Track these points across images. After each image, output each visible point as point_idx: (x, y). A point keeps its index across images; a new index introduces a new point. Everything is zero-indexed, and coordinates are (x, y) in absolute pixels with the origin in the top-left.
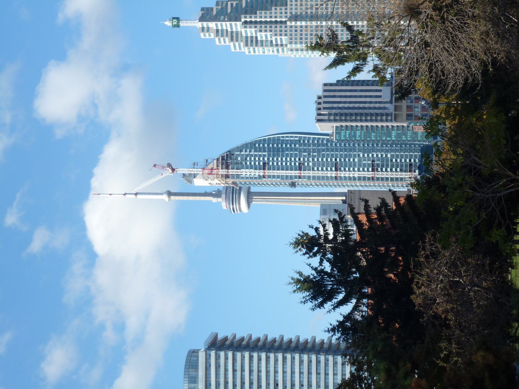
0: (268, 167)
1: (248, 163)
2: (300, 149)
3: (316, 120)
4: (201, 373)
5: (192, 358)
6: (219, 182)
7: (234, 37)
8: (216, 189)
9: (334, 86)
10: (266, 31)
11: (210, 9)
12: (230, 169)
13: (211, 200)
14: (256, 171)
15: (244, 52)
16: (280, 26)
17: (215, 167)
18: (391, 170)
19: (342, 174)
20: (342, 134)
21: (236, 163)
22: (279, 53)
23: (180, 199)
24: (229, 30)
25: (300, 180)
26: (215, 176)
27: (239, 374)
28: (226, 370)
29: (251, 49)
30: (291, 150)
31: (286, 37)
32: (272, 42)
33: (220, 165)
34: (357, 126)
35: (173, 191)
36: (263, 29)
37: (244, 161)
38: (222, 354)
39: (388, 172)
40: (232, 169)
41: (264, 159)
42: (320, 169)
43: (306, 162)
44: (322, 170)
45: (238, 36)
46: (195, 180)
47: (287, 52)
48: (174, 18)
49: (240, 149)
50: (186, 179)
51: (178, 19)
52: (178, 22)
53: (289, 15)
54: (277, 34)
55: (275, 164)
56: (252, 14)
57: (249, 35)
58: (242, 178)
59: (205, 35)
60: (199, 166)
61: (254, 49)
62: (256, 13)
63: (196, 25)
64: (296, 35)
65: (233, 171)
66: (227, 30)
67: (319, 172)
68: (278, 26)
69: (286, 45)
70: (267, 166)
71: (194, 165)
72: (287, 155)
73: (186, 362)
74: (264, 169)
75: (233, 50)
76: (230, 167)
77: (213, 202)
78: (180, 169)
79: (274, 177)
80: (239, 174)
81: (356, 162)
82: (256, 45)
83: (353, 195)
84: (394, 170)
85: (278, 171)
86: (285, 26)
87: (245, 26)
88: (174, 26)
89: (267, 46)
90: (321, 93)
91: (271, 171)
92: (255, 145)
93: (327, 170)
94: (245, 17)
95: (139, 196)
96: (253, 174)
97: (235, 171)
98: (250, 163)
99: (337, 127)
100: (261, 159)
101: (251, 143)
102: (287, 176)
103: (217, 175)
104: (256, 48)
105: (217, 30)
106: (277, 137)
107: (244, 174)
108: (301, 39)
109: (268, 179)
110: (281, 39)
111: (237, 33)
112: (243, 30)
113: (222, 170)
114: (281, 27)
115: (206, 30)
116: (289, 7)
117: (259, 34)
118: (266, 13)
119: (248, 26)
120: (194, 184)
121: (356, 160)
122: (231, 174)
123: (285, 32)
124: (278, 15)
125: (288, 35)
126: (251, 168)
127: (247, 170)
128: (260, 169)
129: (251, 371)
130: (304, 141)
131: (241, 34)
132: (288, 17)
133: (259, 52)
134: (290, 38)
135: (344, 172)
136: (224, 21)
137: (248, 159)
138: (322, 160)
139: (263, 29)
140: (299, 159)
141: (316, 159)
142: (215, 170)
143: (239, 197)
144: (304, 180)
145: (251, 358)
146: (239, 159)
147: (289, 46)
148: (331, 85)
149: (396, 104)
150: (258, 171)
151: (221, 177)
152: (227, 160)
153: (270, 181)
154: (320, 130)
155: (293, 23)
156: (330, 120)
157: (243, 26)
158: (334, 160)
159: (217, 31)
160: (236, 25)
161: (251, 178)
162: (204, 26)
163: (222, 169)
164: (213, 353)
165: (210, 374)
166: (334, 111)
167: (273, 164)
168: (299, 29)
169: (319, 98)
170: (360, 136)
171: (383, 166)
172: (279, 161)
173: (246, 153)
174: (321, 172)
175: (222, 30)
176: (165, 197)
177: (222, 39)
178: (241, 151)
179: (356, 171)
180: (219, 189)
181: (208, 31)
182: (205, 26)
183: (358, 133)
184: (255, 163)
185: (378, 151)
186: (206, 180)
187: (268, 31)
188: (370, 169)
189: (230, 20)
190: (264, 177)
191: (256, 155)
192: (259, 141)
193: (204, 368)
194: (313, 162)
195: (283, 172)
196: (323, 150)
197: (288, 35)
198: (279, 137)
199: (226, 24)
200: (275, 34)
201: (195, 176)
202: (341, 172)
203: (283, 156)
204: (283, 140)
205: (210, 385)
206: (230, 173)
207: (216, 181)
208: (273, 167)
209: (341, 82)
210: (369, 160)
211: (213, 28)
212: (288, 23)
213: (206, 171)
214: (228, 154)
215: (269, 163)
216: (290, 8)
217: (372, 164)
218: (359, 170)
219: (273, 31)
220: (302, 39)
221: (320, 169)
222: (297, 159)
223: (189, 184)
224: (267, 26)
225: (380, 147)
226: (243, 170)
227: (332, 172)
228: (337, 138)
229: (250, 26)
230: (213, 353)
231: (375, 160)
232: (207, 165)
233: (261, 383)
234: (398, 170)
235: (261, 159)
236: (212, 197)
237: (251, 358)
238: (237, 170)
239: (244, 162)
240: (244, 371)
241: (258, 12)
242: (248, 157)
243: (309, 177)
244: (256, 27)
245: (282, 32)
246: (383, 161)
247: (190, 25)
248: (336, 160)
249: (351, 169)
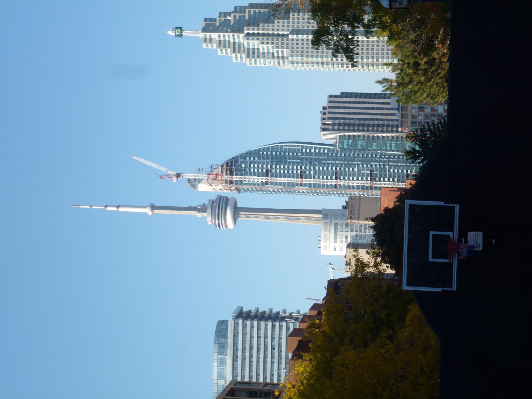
0: (271, 174)
1: (252, 170)
2: (302, 158)
3: (320, 129)
4: (230, 340)
5: (222, 327)
6: (222, 188)
7: (236, 48)
8: (202, 204)
9: (339, 97)
10: (268, 43)
11: (213, 20)
12: (234, 175)
13: (196, 215)
14: (259, 177)
15: (246, 64)
16: (282, 39)
17: (220, 173)
18: (389, 180)
19: (342, 183)
20: (345, 143)
21: (241, 170)
22: (280, 65)
23: (163, 213)
24: (232, 41)
25: (301, 187)
26: (219, 182)
27: (262, 340)
28: (251, 337)
29: (253, 60)
30: (294, 158)
31: (288, 50)
32: (273, 54)
33: (225, 172)
34: (359, 136)
35: (155, 205)
36: (265, 41)
37: (247, 168)
38: (248, 322)
39: (386, 182)
40: (237, 175)
41: (267, 166)
42: (321, 177)
43: (307, 170)
44: (323, 178)
45: (240, 47)
46: (200, 185)
47: (288, 65)
48: (177, 28)
49: (243, 156)
50: (190, 184)
51: (181, 28)
52: (181, 32)
53: (291, 28)
54: (278, 47)
55: (278, 171)
56: (255, 26)
57: (251, 46)
58: (245, 184)
59: (207, 46)
60: (204, 172)
61: (255, 60)
62: (258, 26)
63: (199, 36)
64: (297, 48)
65: (237, 177)
66: (229, 41)
67: (320, 180)
68: (280, 39)
69: (287, 58)
70: (270, 173)
71: (200, 170)
72: (289, 163)
73: (216, 330)
74: (267, 176)
75: (234, 60)
76: (234, 173)
77: (198, 216)
78: (187, 174)
79: (276, 184)
80: (243, 180)
81: (355, 171)
82: (258, 57)
83: (354, 201)
84: (391, 180)
85: (280, 179)
86: (287, 39)
87: (247, 38)
88: (177, 36)
89: (268, 58)
90: (326, 104)
91: (274, 178)
93: (327, 178)
94: (248, 29)
95: (121, 209)
96: (256, 180)
97: (239, 177)
98: (254, 170)
99: (340, 136)
100: (265, 166)
101: (255, 151)
102: (289, 184)
103: (221, 181)
104: (258, 60)
105: (219, 41)
106: (281, 146)
107: (247, 180)
108: (302, 52)
109: (271, 186)
110: (282, 51)
111: (239, 44)
112: (246, 42)
113: (227, 176)
114: (283, 40)
115: (208, 40)
116: (291, 20)
117: (260, 46)
118: (268, 26)
119: (250, 38)
120: (198, 189)
121: (356, 169)
122: (235, 180)
123: (287, 44)
124: (281, 28)
125: (290, 48)
126: (255, 175)
127: (250, 177)
128: (263, 176)
129: (273, 338)
131: (244, 46)
132: (290, 30)
133: (260, 64)
134: (291, 51)
135: (344, 181)
136: (227, 32)
137: (252, 166)
138: (323, 168)
139: (265, 41)
140: (301, 168)
141: (317, 168)
142: (219, 176)
143: (226, 213)
144: (305, 187)
145: (273, 327)
146: (243, 166)
147: (290, 58)
148: (336, 96)
149: (402, 112)
150: (261, 177)
151: (225, 183)
152: (232, 166)
153: (272, 188)
154: (324, 139)
155: (295, 37)
156: (334, 130)
157: (246, 37)
158: (334, 169)
159: (220, 42)
160: (238, 36)
161: (254, 184)
162: (206, 37)
163: (226, 175)
164: (240, 322)
165: (237, 340)
166: (337, 121)
167: (276, 171)
168: (300, 42)
169: (325, 108)
170: (362, 145)
171: (381, 176)
172: (282, 169)
173: (250, 160)
174: (322, 180)
175: (225, 41)
176: (148, 211)
177: (224, 50)
178: (245, 158)
179: (355, 180)
180: (204, 204)
181: (210, 41)
182: (208, 37)
183: (360, 142)
184: (258, 170)
185: (377, 161)
186: (210, 185)
187: (270, 43)
188: (369, 179)
189: (233, 31)
190: (267, 183)
192: (263, 149)
193: (233, 335)
194: (314, 170)
195: (285, 179)
196: (324, 159)
197: (290, 48)
198: (282, 145)
199: (229, 35)
200: (276, 47)
201: (200, 181)
202: (341, 181)
203: (285, 164)
204: (285, 149)
205: (237, 349)
206: (234, 179)
207: (220, 187)
208: (275, 175)
209: (345, 94)
210: (368, 170)
211: (215, 39)
212: (290, 36)
213: (211, 177)
214: (233, 161)
215: (272, 170)
216: (292, 22)
217: (371, 173)
218: (358, 179)
219: (275, 43)
220: (303, 53)
221: (321, 177)
222: (299, 167)
223: (193, 189)
224: (269, 39)
225: (378, 158)
226: (246, 177)
227: (332, 181)
228: (340, 147)
229: (252, 38)
230: (240, 322)
231: (373, 170)
232: (211, 171)
233: (282, 348)
234: (396, 180)
235: (265, 166)
236: (197, 212)
237: (273, 327)
238: (241, 177)
239: (247, 169)
240: (267, 338)
241: (261, 25)
242: (252, 164)
243: (310, 185)
244: (258, 39)
245: (284, 44)
246: (381, 171)
247: (192, 35)
248: (336, 169)
249: (351, 178)
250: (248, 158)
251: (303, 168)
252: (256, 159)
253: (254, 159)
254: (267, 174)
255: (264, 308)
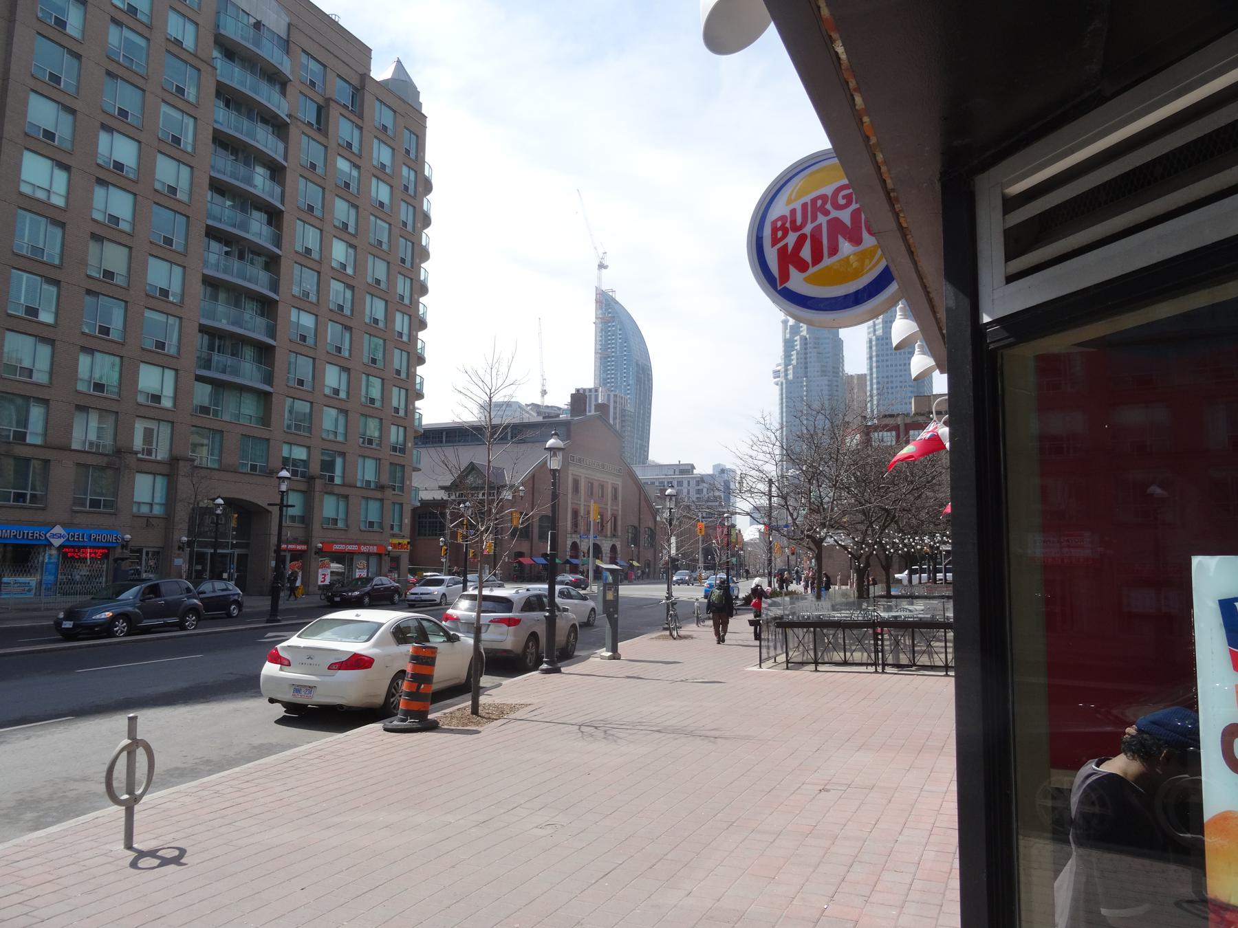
30: (621, 378)
41: (613, 352)
72: (616, 374)
92: (625, 342)
130: (628, 389)
137: (613, 337)
140: (612, 386)
178: (620, 330)
191: (616, 345)
222: (613, 384)
235: (613, 350)
250: (620, 332)
251: (612, 389)
252: (620, 341)
253: (620, 338)
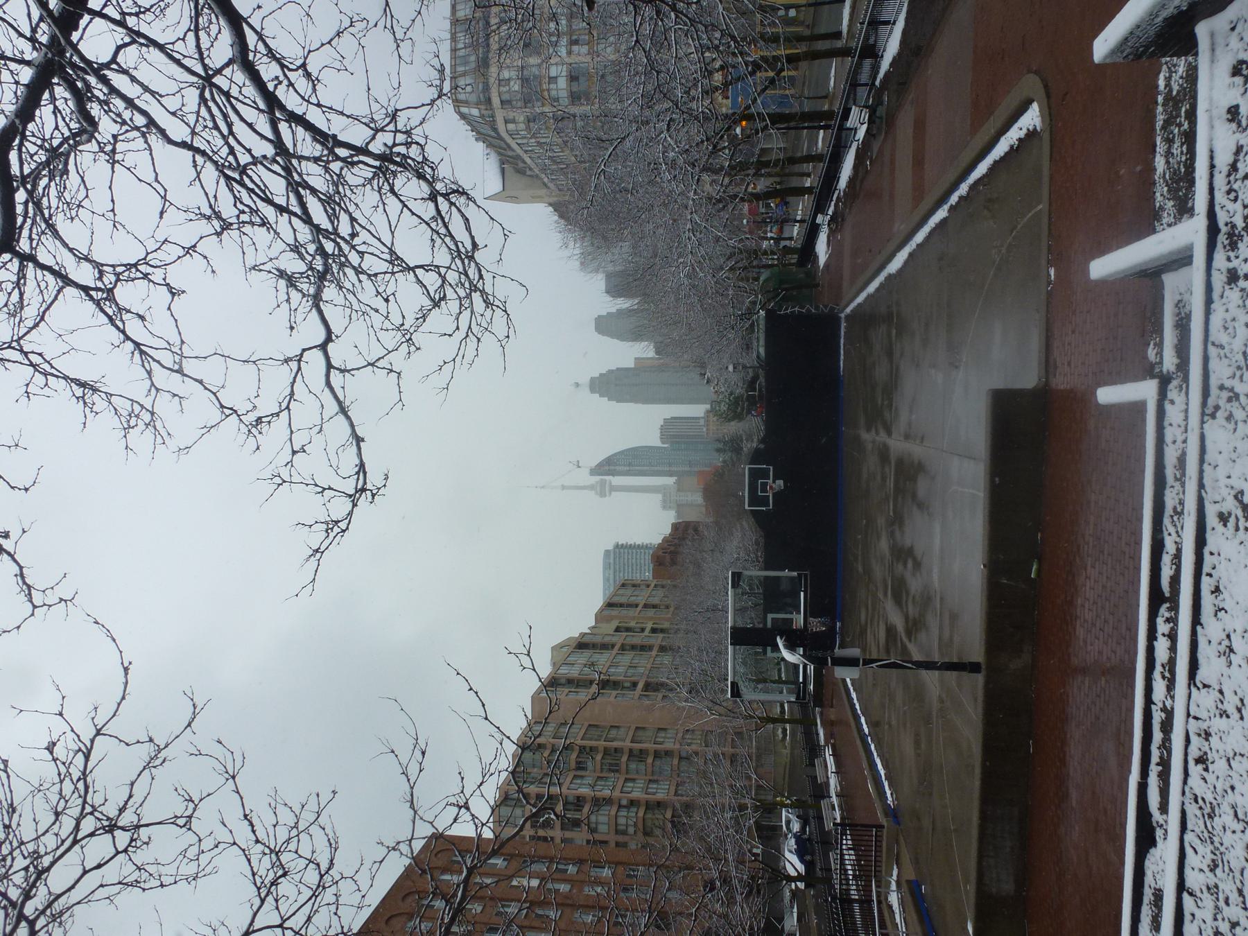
27: (630, 561)
35: (565, 484)
49: (615, 455)
164: (617, 550)
230: (617, 550)
254: (630, 465)
255: (631, 542)
